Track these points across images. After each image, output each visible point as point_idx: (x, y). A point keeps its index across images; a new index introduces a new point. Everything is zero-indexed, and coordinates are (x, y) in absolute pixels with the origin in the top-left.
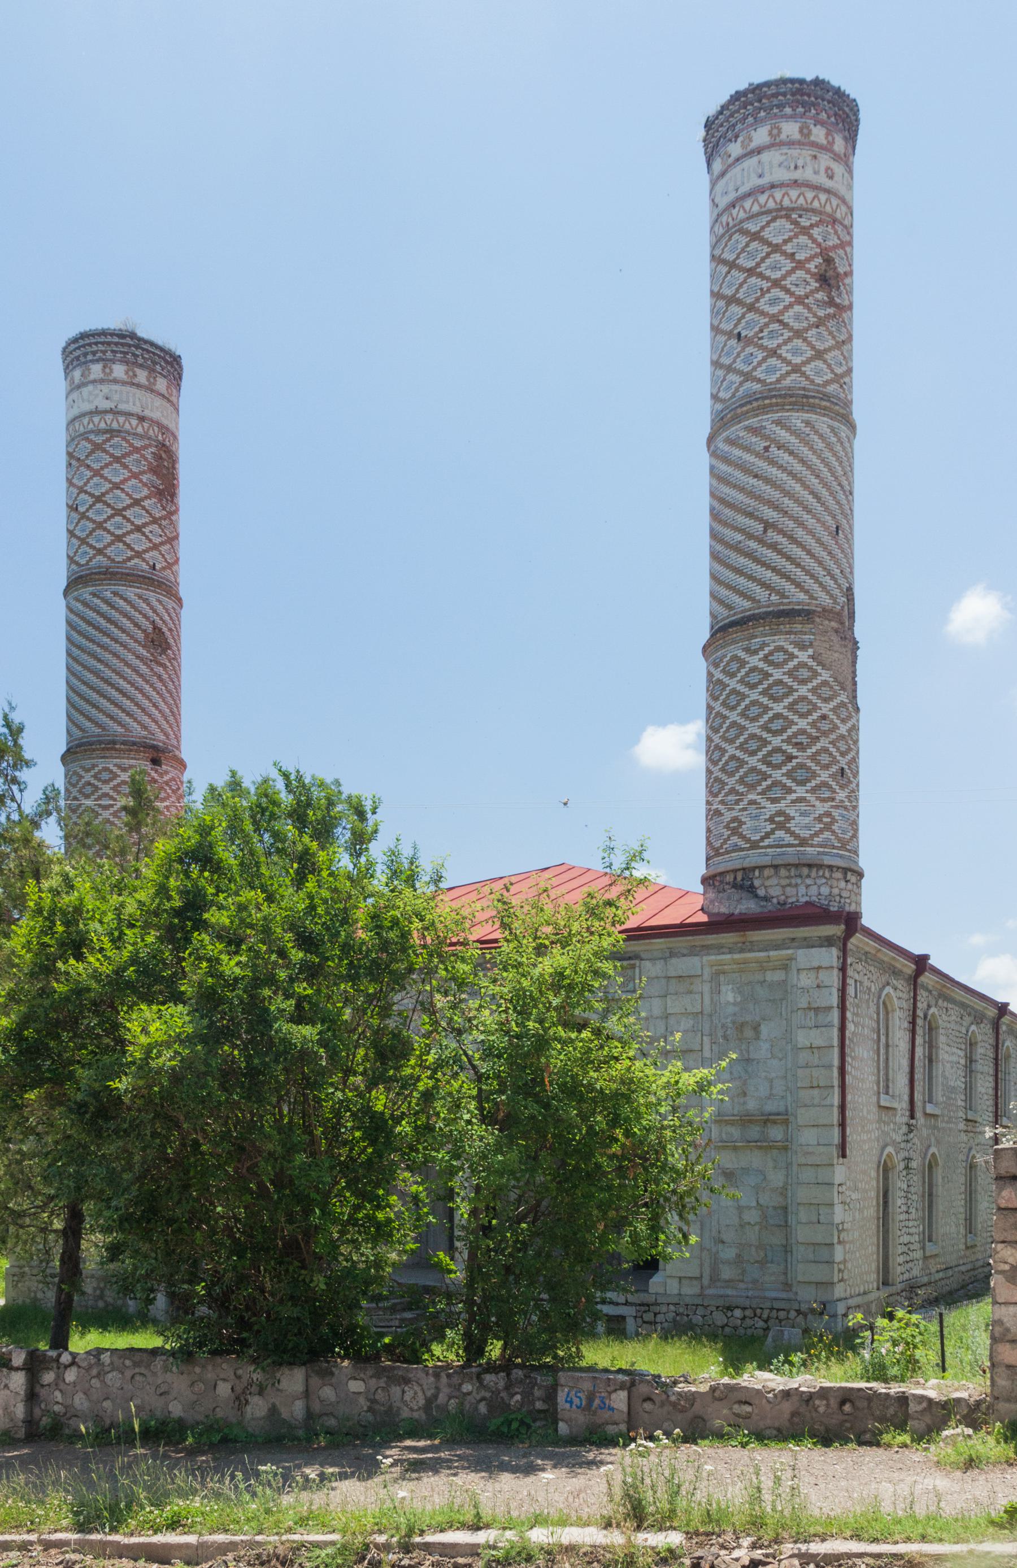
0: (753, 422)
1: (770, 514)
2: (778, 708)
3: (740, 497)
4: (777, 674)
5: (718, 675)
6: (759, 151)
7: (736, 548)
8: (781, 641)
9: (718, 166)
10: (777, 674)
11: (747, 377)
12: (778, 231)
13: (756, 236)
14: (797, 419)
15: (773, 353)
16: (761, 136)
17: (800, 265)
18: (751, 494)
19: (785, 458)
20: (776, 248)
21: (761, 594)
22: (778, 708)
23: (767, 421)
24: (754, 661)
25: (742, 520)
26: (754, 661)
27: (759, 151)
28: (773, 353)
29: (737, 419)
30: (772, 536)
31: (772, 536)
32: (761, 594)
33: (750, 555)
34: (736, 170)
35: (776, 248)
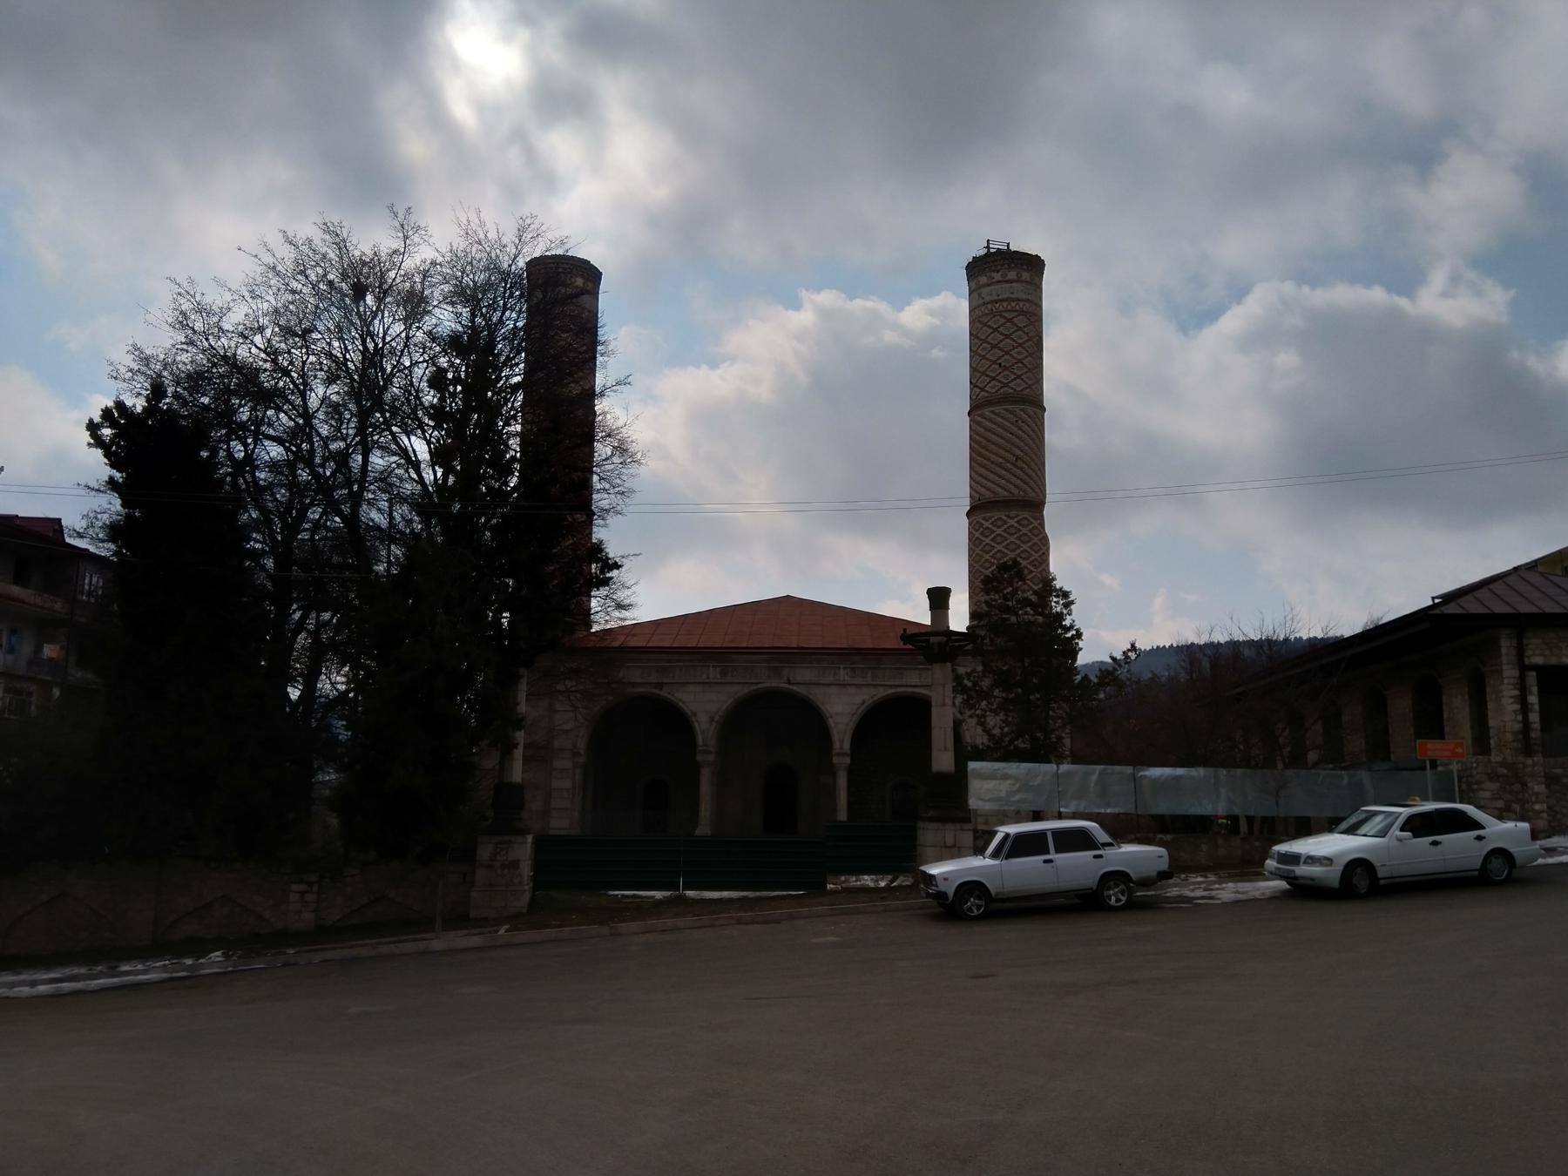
0: (1010, 407)
1: (1018, 452)
2: (1025, 547)
3: (1001, 441)
4: (1024, 530)
5: (986, 524)
6: (1011, 281)
7: (999, 465)
8: (1026, 515)
9: (983, 280)
10: (1024, 530)
11: (1006, 385)
12: (1021, 321)
13: (1009, 320)
14: (1030, 410)
15: (1019, 377)
16: (1012, 275)
17: (1030, 339)
18: (1008, 441)
19: (1025, 427)
20: (1020, 329)
21: (1016, 491)
22: (1025, 547)
23: (1017, 408)
24: (1012, 522)
25: (1002, 453)
26: (1012, 522)
27: (1011, 281)
28: (1019, 377)
29: (999, 402)
30: (1020, 463)
31: (1020, 463)
32: (1016, 491)
33: (1007, 470)
34: (998, 286)
35: (1020, 329)
